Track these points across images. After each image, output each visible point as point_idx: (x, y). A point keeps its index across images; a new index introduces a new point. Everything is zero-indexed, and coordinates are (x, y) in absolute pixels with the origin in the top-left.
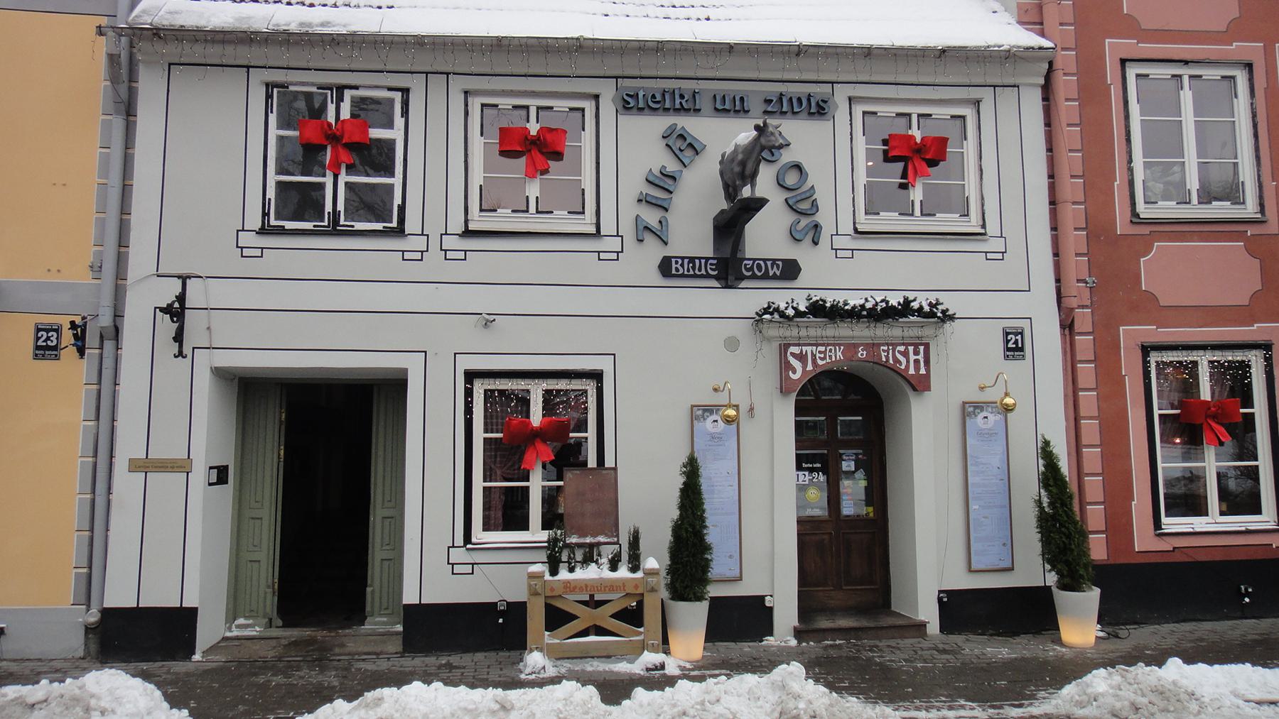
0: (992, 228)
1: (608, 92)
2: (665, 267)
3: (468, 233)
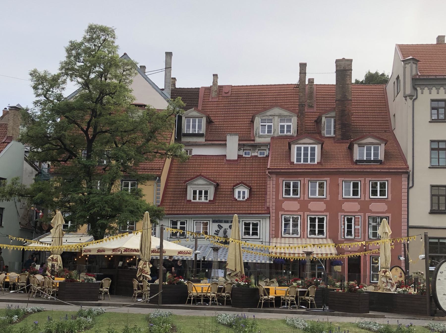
0: (261, 238)
1: (211, 220)
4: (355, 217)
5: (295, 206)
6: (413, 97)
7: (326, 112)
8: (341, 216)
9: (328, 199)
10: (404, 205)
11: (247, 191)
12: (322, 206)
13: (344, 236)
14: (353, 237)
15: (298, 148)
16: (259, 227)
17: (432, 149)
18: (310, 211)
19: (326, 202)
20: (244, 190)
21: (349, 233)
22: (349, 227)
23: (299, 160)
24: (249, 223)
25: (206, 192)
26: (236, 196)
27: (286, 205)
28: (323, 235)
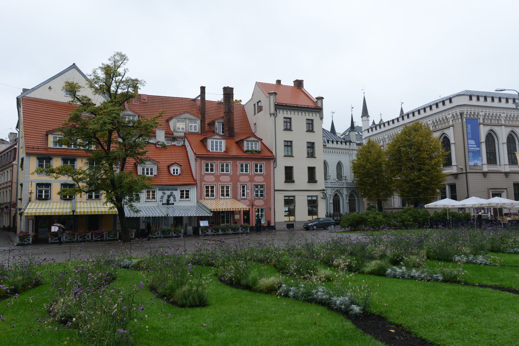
0: (191, 200)
1: (157, 189)
2: (163, 204)
3: (145, 202)
4: (246, 185)
5: (211, 179)
6: (275, 115)
7: (219, 119)
8: (239, 185)
9: (231, 174)
10: (272, 177)
11: (179, 169)
12: (228, 179)
13: (241, 197)
14: (245, 197)
15: (211, 141)
16: (190, 193)
17: (285, 146)
18: (221, 182)
19: (231, 176)
20: (177, 168)
21: (243, 195)
22: (243, 191)
23: (212, 149)
24: (184, 190)
25: (152, 170)
26: (172, 172)
27: (206, 178)
28: (229, 196)
